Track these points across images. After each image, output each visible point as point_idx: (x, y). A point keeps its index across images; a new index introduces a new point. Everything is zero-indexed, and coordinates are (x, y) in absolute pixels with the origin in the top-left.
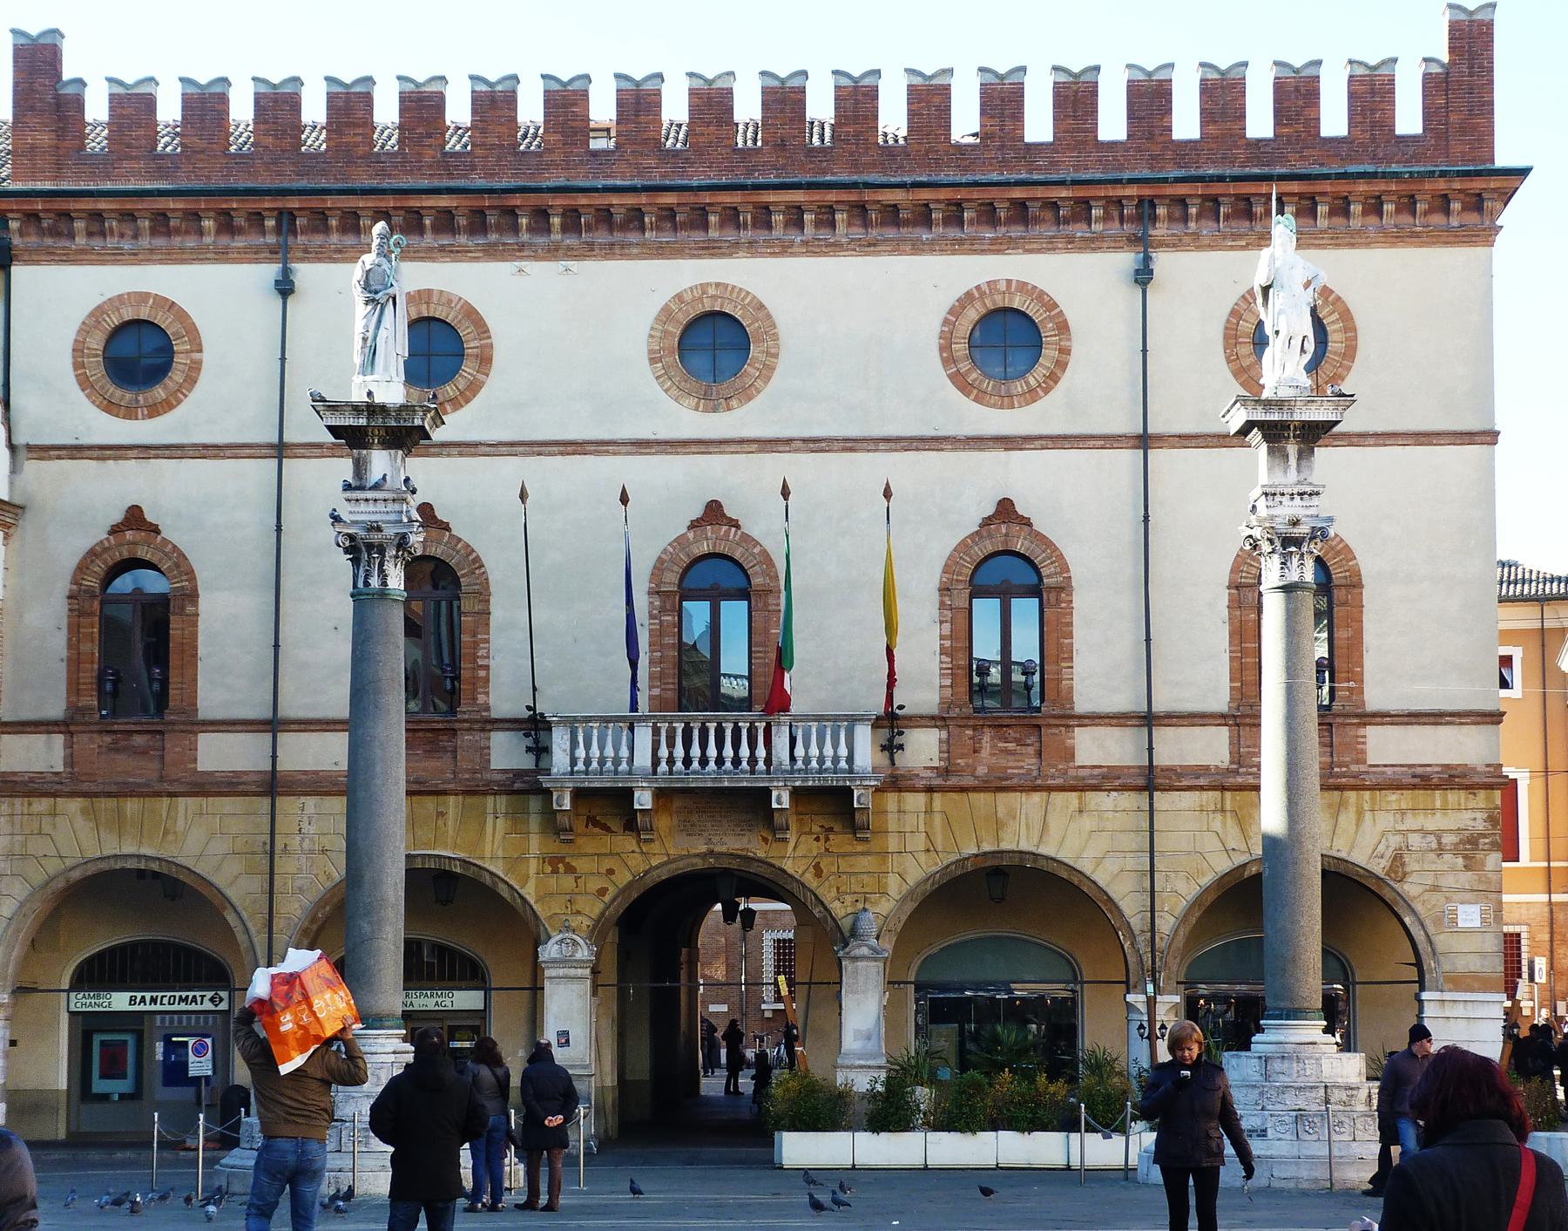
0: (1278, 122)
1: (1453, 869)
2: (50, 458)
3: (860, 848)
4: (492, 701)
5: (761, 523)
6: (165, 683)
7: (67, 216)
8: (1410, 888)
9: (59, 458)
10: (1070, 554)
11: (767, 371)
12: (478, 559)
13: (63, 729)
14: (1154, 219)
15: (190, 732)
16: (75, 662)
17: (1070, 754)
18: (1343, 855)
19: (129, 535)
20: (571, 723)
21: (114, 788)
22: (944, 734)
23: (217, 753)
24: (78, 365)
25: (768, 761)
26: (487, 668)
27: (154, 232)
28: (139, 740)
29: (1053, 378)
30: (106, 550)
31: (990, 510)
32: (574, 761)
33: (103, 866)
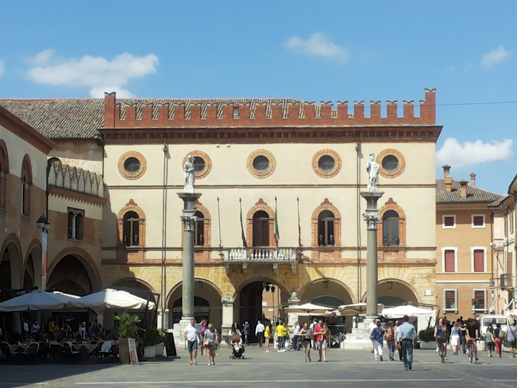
0: (388, 114)
1: (425, 282)
3: (293, 277)
4: (211, 244)
5: (271, 205)
7: (117, 134)
8: (416, 286)
10: (341, 211)
11: (273, 169)
12: (208, 211)
14: (360, 136)
17: (340, 256)
18: (400, 279)
19: (130, 206)
20: (229, 250)
22: (312, 252)
23: (150, 256)
24: (119, 168)
25: (272, 257)
26: (210, 236)
27: (136, 138)
29: (337, 172)
30: (126, 209)
31: (323, 201)
32: (229, 258)
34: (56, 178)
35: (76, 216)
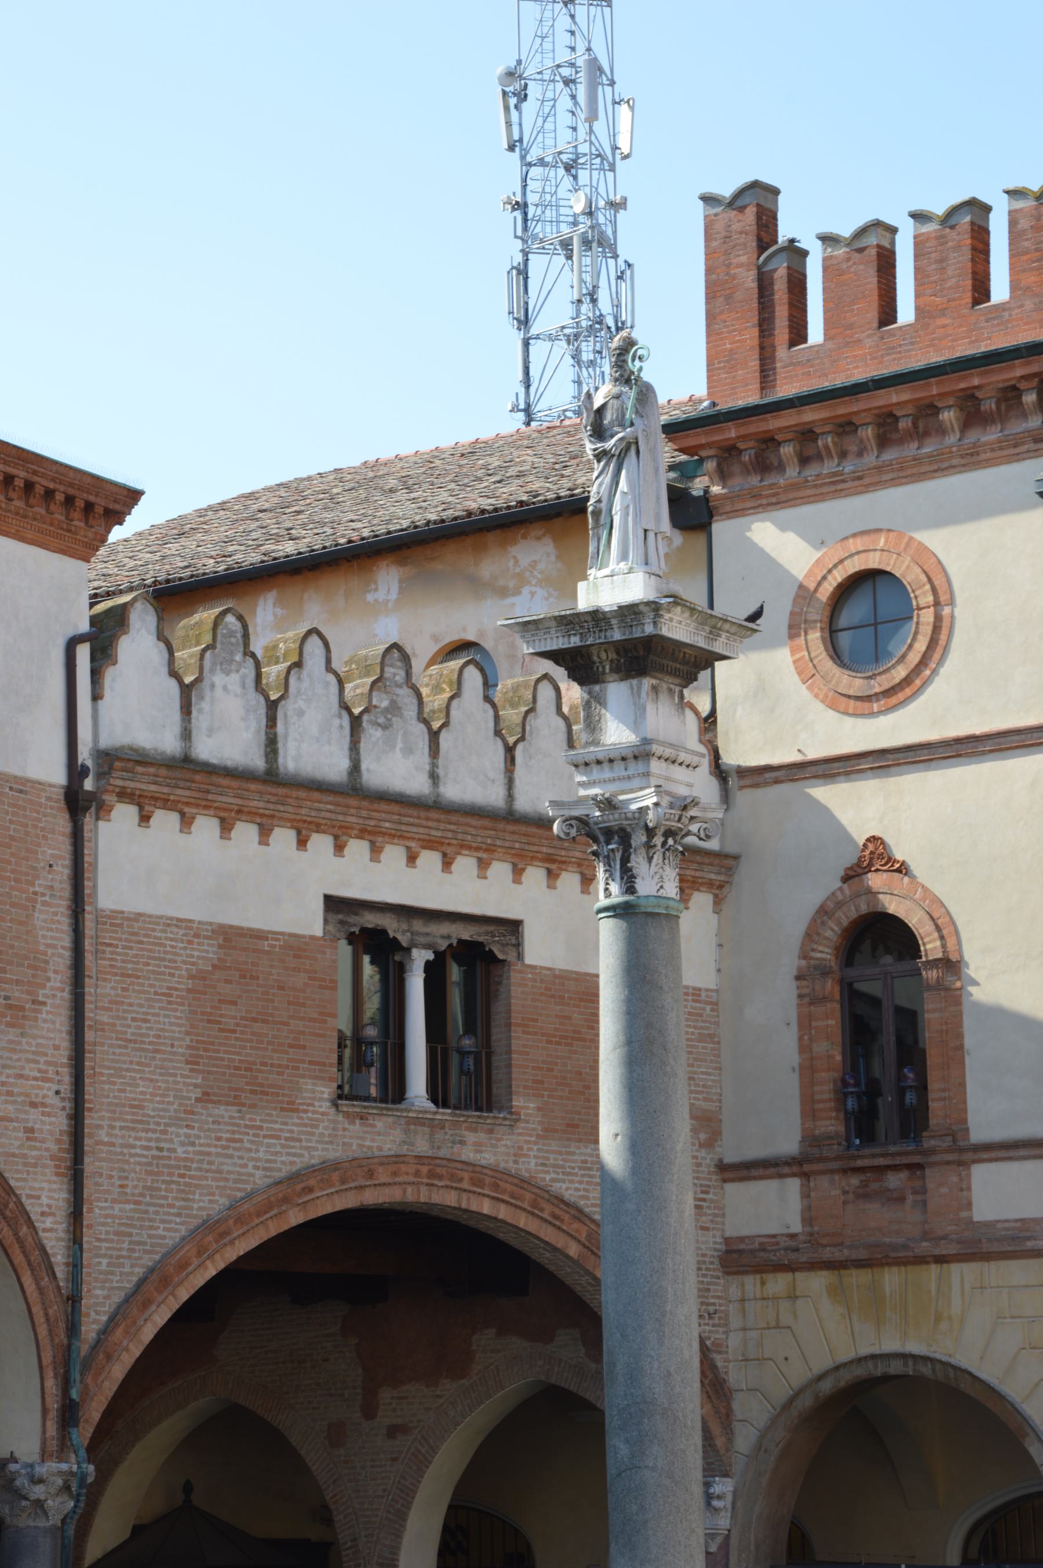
2: (766, 784)
6: (922, 1087)
7: (770, 441)
9: (777, 781)
13: (795, 1169)
15: (960, 1163)
16: (808, 1071)
21: (862, 1254)
28: (895, 1180)
30: (840, 904)
33: (859, 1372)
34: (186, 709)
35: (420, 957)
